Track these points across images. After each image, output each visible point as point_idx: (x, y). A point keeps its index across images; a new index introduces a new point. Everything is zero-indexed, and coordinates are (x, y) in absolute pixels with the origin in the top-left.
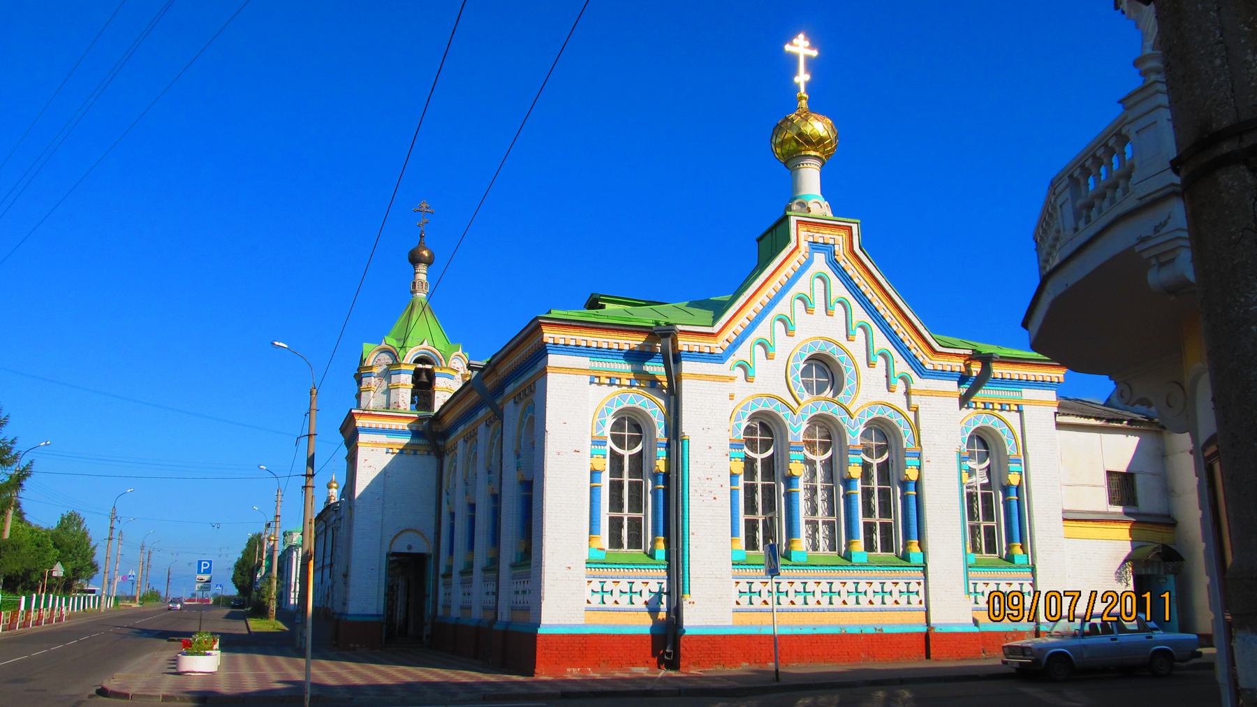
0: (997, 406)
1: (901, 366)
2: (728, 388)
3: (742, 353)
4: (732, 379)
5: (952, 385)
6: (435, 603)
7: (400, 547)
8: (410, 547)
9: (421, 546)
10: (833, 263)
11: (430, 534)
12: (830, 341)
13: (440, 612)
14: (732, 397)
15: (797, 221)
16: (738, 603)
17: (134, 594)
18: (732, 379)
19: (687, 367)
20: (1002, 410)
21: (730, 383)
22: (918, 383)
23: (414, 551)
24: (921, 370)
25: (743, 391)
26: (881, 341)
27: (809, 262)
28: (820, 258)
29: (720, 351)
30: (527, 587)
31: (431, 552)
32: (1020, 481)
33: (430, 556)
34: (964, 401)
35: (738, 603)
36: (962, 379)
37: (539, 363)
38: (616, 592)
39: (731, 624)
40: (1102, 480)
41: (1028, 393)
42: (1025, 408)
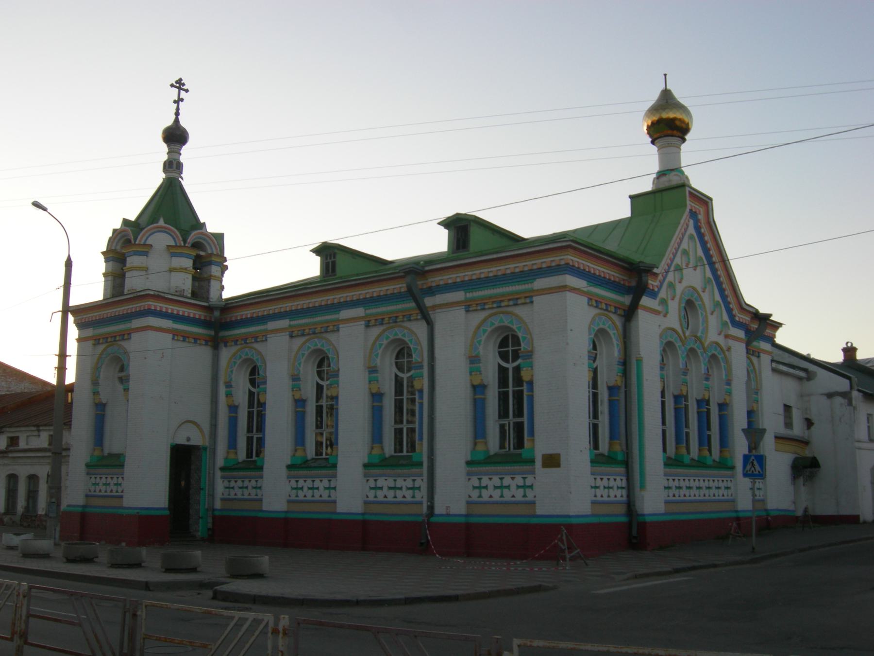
1: (726, 317)
2: (658, 319)
5: (741, 334)
6: (212, 496)
7: (181, 440)
8: (188, 439)
9: (197, 439)
10: (698, 228)
11: (206, 426)
12: (694, 289)
13: (218, 505)
14: (660, 326)
23: (192, 443)
28: (691, 222)
30: (729, 484)
31: (207, 444)
33: (205, 449)
36: (748, 331)
37: (538, 280)
39: (664, 512)
42: (762, 355)
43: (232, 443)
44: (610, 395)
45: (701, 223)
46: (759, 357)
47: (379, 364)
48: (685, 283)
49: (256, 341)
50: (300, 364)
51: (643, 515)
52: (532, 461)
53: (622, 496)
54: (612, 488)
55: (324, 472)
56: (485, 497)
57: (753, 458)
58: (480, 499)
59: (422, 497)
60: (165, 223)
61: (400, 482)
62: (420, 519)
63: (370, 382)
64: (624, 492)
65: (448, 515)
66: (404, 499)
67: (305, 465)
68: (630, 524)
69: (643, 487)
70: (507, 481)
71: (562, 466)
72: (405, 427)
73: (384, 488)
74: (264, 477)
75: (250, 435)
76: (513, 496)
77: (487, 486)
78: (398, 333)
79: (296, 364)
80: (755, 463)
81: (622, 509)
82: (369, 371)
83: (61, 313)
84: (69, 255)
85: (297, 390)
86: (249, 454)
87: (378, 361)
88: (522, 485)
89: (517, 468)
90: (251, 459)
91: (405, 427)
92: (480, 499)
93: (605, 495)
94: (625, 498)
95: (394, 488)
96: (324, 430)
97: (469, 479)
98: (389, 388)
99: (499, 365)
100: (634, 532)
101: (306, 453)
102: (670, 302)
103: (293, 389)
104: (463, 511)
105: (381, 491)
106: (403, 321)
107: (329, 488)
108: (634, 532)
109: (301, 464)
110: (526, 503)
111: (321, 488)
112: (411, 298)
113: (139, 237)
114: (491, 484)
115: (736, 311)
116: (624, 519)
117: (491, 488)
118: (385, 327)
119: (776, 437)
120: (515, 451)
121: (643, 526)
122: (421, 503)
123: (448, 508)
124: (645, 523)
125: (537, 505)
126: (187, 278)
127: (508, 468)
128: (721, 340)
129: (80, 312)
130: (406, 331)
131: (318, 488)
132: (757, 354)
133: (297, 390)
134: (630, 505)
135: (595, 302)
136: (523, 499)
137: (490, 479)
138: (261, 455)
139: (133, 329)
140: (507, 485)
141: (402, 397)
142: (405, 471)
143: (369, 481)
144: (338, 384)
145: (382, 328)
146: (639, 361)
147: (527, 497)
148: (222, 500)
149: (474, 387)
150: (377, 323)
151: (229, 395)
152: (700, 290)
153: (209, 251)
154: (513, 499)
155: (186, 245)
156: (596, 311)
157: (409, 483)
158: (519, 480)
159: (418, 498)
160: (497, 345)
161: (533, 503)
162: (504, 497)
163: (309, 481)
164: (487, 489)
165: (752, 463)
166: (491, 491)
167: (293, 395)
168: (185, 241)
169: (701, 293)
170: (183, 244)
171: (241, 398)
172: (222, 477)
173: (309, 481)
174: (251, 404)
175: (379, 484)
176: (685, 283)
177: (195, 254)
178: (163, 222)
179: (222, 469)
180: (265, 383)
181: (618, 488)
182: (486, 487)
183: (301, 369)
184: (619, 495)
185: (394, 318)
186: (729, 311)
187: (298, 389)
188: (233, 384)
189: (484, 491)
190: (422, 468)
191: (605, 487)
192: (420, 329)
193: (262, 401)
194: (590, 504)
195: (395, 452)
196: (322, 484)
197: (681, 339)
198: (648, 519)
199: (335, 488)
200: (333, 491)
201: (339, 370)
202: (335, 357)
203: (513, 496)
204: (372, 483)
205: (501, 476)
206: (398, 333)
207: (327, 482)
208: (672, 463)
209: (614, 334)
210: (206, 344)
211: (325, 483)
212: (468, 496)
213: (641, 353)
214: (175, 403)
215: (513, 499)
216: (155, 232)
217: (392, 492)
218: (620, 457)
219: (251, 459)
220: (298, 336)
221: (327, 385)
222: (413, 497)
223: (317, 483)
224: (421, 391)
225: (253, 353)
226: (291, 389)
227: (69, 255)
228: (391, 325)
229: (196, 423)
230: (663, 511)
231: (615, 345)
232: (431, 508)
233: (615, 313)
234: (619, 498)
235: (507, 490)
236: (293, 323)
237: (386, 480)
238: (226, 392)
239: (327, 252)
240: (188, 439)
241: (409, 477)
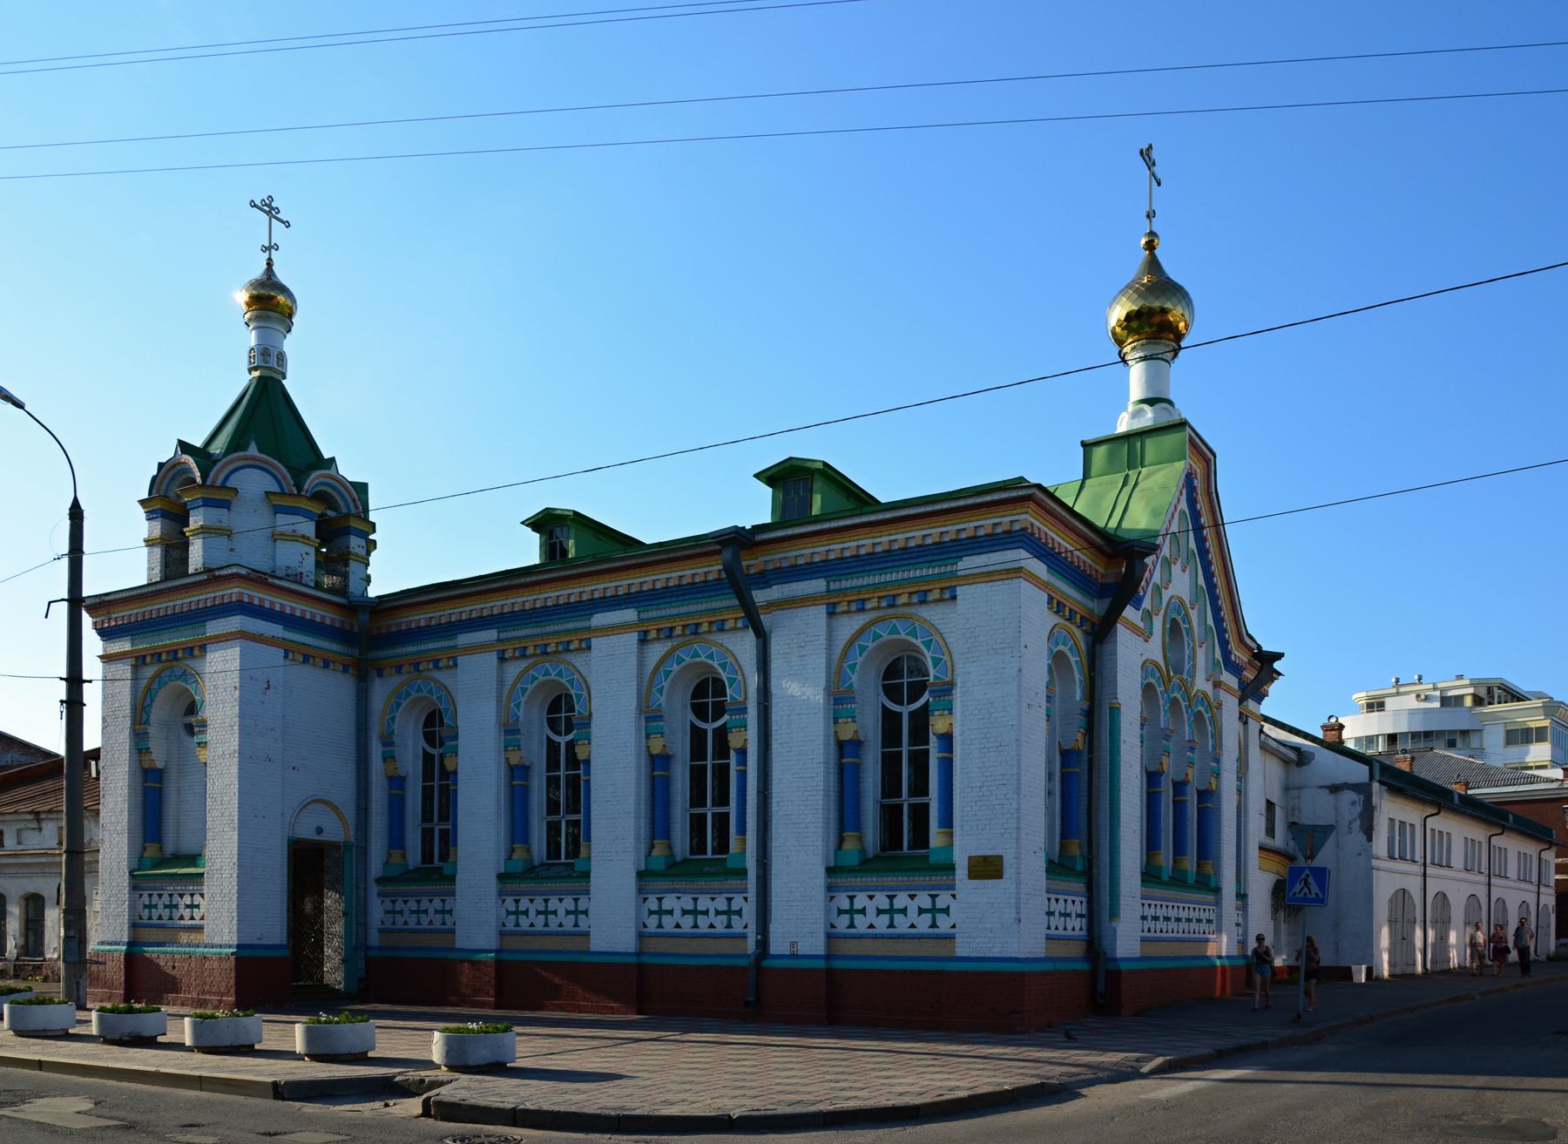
7: (306, 832)
47: (664, 705)
49: (437, 667)
50: (518, 706)
51: (1115, 960)
52: (950, 868)
53: (1081, 929)
54: (1061, 914)
55: (566, 885)
58: (852, 931)
59: (746, 927)
61: (704, 903)
62: (743, 962)
63: (648, 736)
65: (794, 956)
66: (712, 930)
67: (531, 872)
68: (1093, 974)
70: (901, 900)
71: (1005, 876)
72: (709, 811)
73: (675, 911)
74: (457, 894)
75: (427, 825)
76: (912, 926)
77: (906, 909)
78: (703, 653)
79: (512, 705)
81: (1077, 950)
82: (646, 718)
85: (513, 750)
86: (427, 856)
87: (663, 700)
88: (930, 907)
89: (918, 879)
90: (559, 861)
91: (709, 811)
92: (852, 931)
93: (1061, 927)
95: (695, 912)
96: (563, 817)
97: (832, 898)
98: (681, 748)
99: (884, 707)
100: (1101, 986)
101: (531, 855)
103: (506, 747)
104: (821, 950)
105: (670, 916)
106: (709, 632)
107: (576, 912)
108: (1101, 986)
109: (523, 873)
110: (937, 937)
111: (561, 912)
112: (734, 596)
114: (871, 907)
116: (1084, 966)
117: (871, 912)
118: (675, 644)
120: (910, 852)
121: (1115, 976)
122: (744, 937)
123: (793, 944)
124: (1119, 972)
125: (956, 940)
126: (307, 554)
127: (903, 879)
129: (101, 605)
130: (714, 649)
131: (555, 913)
133: (513, 750)
134: (1094, 944)
135: (1057, 606)
136: (931, 930)
137: (871, 897)
138: (451, 859)
139: (211, 638)
140: (902, 907)
141: (899, 749)
142: (715, 884)
143: (648, 901)
144: (589, 740)
145: (669, 645)
147: (855, 927)
149: (841, 745)
150: (662, 636)
153: (344, 510)
154: (913, 931)
157: (721, 904)
158: (924, 900)
159: (737, 927)
160: (881, 678)
161: (951, 937)
162: (895, 927)
163: (539, 901)
164: (865, 915)
166: (871, 916)
167: (507, 759)
171: (410, 764)
173: (539, 901)
174: (428, 774)
175: (666, 905)
180: (456, 737)
182: (863, 911)
183: (521, 714)
184: (1076, 926)
185: (693, 626)
187: (516, 748)
188: (396, 740)
189: (858, 918)
190: (746, 879)
192: (743, 646)
193: (449, 767)
194: (1044, 941)
195: (691, 854)
198: (1123, 966)
199: (585, 912)
200: (582, 917)
201: (590, 715)
202: (585, 693)
203: (912, 926)
204: (652, 904)
205: (890, 893)
206: (703, 653)
207: (572, 901)
208: (1150, 875)
210: (345, 670)
211: (569, 903)
212: (829, 926)
214: (294, 768)
215: (913, 931)
217: (689, 919)
219: (559, 861)
220: (514, 658)
221: (567, 743)
222: (729, 926)
223: (553, 904)
224: (742, 752)
225: (431, 688)
226: (503, 749)
228: (687, 638)
229: (332, 804)
232: (763, 943)
234: (1077, 932)
235: (861, 915)
236: (503, 635)
237: (679, 898)
238: (383, 753)
241: (721, 893)
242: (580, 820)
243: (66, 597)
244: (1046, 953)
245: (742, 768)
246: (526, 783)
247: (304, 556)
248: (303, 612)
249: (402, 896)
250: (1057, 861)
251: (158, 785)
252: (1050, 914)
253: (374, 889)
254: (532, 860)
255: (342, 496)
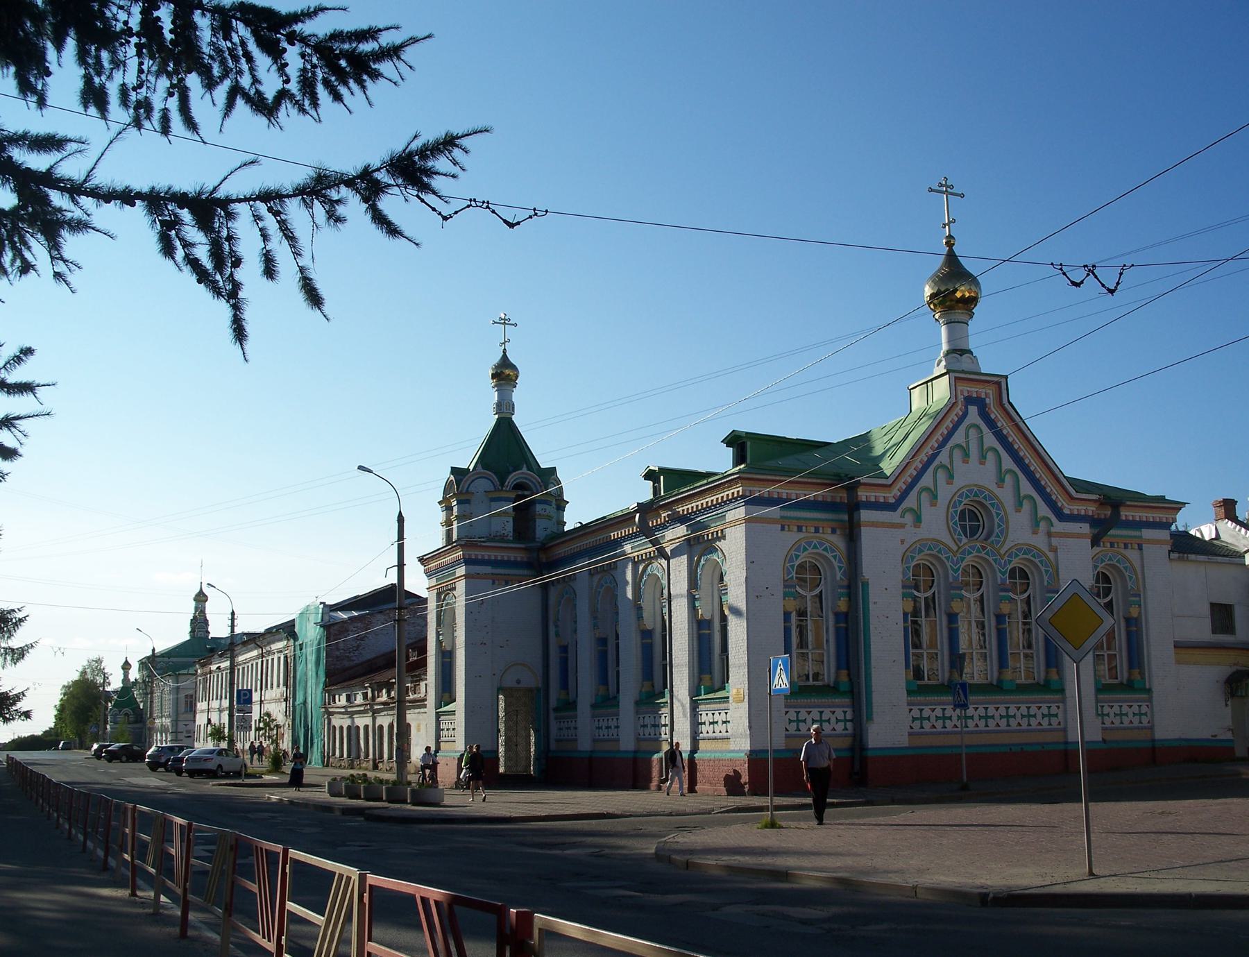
0: (1122, 546)
1: (1043, 510)
3: (910, 502)
4: (902, 526)
5: (1085, 528)
10: (984, 414)
13: (553, 746)
14: (902, 542)
15: (955, 377)
16: (911, 728)
17: (606, 730)
18: (902, 526)
19: (865, 515)
20: (1126, 546)
21: (903, 530)
22: (1059, 526)
24: (1061, 516)
25: (912, 535)
26: (1026, 488)
27: (965, 414)
28: (973, 410)
29: (892, 501)
31: (540, 685)
32: (1140, 613)
34: (1095, 542)
35: (911, 728)
36: (1093, 521)
38: (833, 720)
39: (907, 745)
40: (1206, 610)
41: (1147, 533)
43: (564, 684)
44: (837, 621)
45: (989, 409)
46: (1140, 548)
48: (959, 482)
56: (1126, 723)
57: (959, 686)
60: (483, 469)
64: (849, 725)
69: (870, 718)
80: (960, 691)
83: (396, 568)
84: (400, 511)
94: (850, 730)
102: (927, 513)
113: (461, 486)
115: (1062, 502)
119: (1178, 646)
128: (1040, 541)
132: (1136, 546)
146: (866, 585)
148: (558, 741)
151: (557, 635)
152: (993, 487)
155: (504, 489)
156: (792, 537)
165: (958, 691)
168: (502, 484)
169: (997, 491)
170: (500, 488)
172: (556, 718)
176: (959, 482)
177: (514, 496)
178: (481, 468)
179: (556, 710)
181: (704, 723)
186: (1052, 505)
191: (611, 727)
194: (784, 738)
196: (612, 723)
197: (950, 549)
198: (870, 754)
203: (720, 732)
209: (835, 557)
213: (864, 574)
216: (477, 479)
218: (844, 687)
227: (400, 511)
230: (906, 744)
231: (837, 569)
233: (834, 531)
239: (650, 475)
240: (518, 682)
242: (913, 648)
243: (397, 564)
244: (786, 746)
245: (788, 624)
246: (606, 648)
247: (506, 523)
248: (508, 557)
249: (805, 707)
250: (946, 684)
251: (445, 660)
252: (454, 729)
253: (552, 715)
254: (609, 695)
255: (532, 482)
